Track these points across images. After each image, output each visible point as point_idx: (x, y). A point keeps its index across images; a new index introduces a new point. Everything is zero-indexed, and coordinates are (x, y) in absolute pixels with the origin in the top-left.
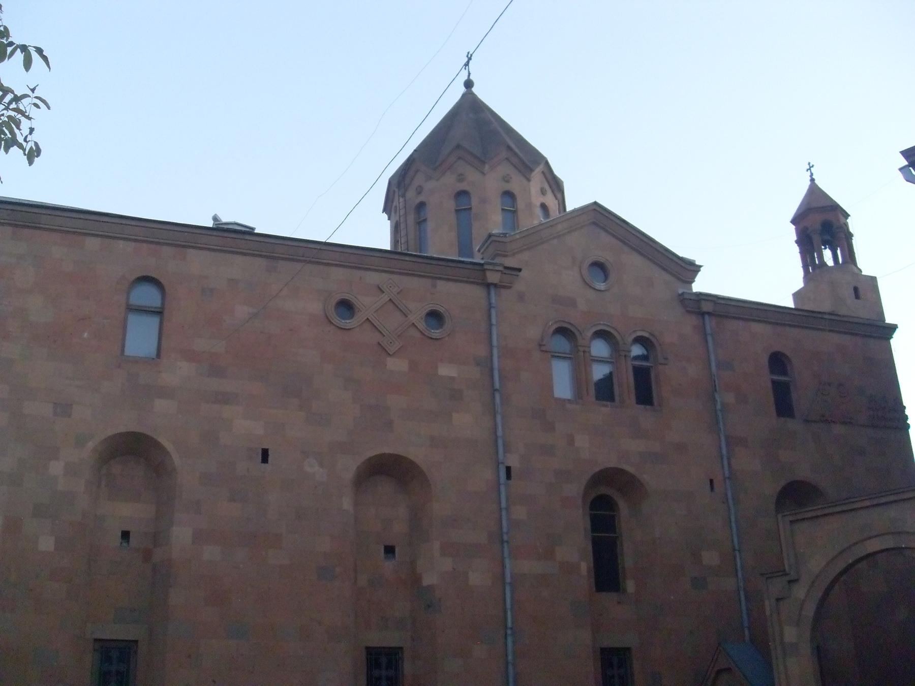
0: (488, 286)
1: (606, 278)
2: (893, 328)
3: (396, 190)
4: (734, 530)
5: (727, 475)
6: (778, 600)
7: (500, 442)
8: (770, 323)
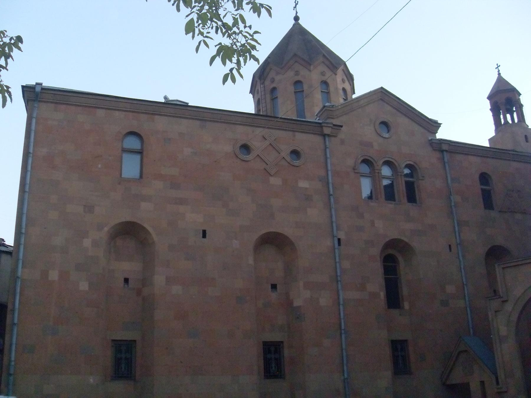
0: (324, 136)
1: (388, 131)
3: (258, 81)
4: (463, 274)
5: (458, 241)
6: (496, 312)
7: (334, 225)
8: (478, 156)
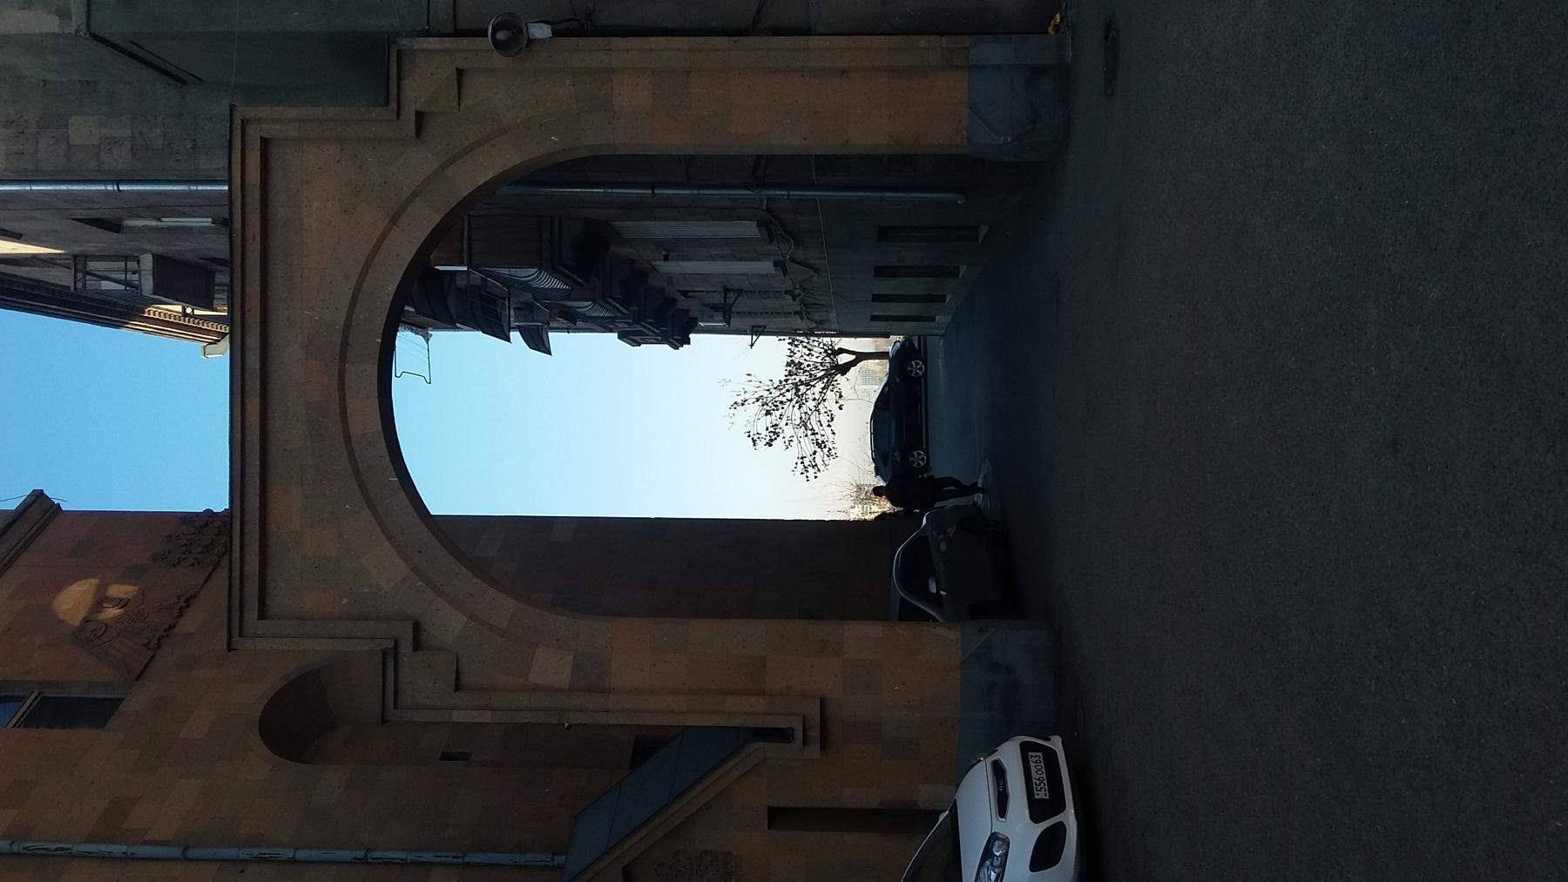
2: (38, 497)
6: (457, 689)
